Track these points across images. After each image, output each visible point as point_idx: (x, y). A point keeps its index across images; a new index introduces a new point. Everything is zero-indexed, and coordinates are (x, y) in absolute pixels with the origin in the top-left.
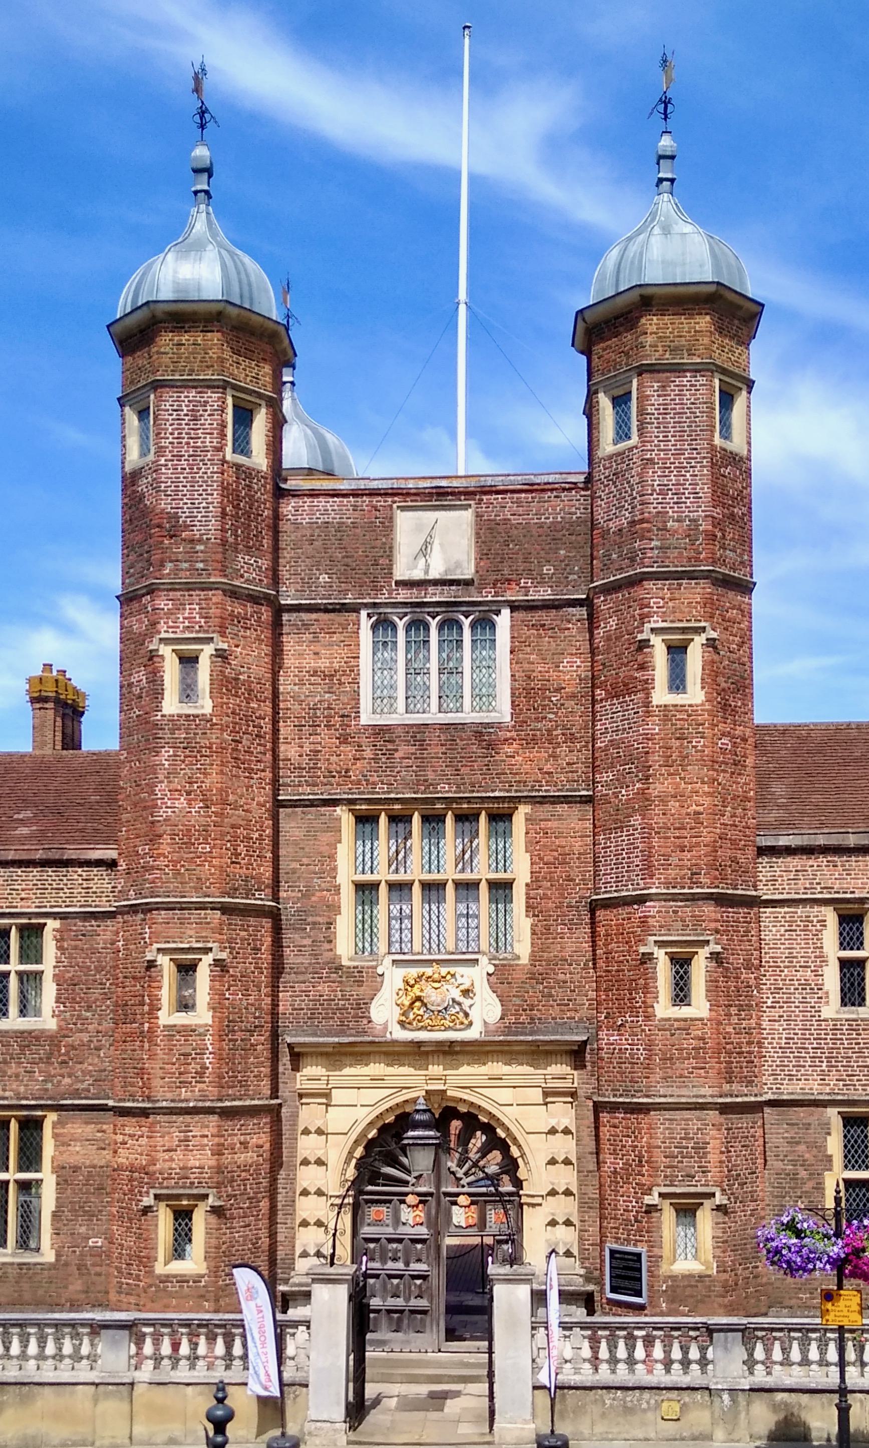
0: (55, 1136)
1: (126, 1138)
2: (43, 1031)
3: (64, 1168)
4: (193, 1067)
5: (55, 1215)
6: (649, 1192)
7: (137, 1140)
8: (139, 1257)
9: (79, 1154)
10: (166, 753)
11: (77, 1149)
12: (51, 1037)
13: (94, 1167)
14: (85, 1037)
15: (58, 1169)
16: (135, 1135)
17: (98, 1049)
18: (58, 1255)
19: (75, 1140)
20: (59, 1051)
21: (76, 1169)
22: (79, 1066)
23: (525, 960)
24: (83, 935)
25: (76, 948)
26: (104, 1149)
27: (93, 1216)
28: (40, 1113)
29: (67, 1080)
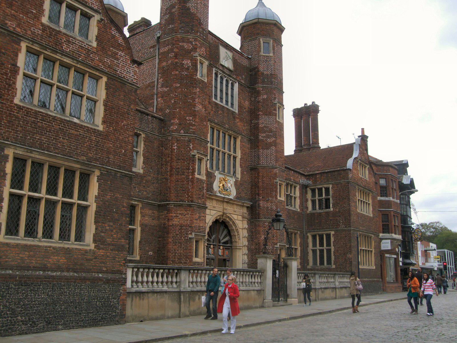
0: (141, 213)
1: (178, 215)
2: (139, 173)
3: (143, 225)
4: (202, 193)
5: (140, 242)
6: (276, 244)
7: (185, 216)
8: (186, 256)
9: (148, 220)
10: (198, 90)
11: (147, 218)
12: (141, 176)
13: (151, 225)
14: (150, 178)
15: (142, 225)
16: (183, 214)
17: (153, 183)
18: (140, 258)
19: (146, 215)
20: (143, 182)
21: (146, 226)
22: (148, 188)
23: (239, 180)
24: (151, 142)
25: (149, 146)
26: (154, 220)
27: (150, 243)
28: (136, 203)
29: (145, 193)
